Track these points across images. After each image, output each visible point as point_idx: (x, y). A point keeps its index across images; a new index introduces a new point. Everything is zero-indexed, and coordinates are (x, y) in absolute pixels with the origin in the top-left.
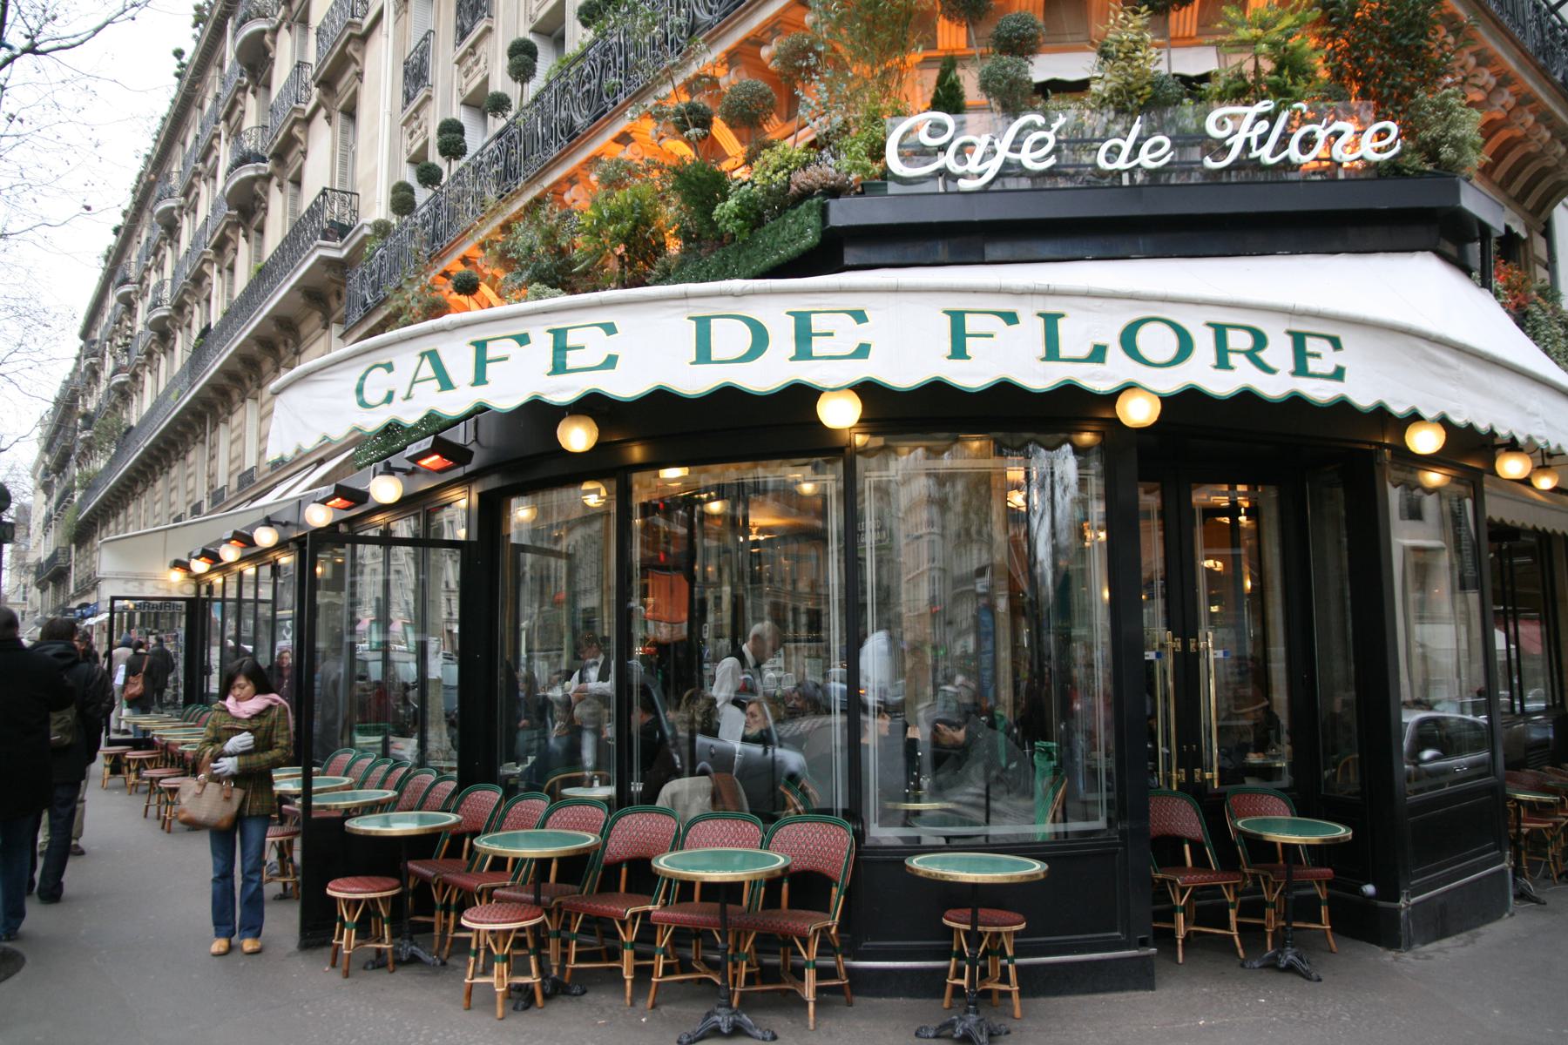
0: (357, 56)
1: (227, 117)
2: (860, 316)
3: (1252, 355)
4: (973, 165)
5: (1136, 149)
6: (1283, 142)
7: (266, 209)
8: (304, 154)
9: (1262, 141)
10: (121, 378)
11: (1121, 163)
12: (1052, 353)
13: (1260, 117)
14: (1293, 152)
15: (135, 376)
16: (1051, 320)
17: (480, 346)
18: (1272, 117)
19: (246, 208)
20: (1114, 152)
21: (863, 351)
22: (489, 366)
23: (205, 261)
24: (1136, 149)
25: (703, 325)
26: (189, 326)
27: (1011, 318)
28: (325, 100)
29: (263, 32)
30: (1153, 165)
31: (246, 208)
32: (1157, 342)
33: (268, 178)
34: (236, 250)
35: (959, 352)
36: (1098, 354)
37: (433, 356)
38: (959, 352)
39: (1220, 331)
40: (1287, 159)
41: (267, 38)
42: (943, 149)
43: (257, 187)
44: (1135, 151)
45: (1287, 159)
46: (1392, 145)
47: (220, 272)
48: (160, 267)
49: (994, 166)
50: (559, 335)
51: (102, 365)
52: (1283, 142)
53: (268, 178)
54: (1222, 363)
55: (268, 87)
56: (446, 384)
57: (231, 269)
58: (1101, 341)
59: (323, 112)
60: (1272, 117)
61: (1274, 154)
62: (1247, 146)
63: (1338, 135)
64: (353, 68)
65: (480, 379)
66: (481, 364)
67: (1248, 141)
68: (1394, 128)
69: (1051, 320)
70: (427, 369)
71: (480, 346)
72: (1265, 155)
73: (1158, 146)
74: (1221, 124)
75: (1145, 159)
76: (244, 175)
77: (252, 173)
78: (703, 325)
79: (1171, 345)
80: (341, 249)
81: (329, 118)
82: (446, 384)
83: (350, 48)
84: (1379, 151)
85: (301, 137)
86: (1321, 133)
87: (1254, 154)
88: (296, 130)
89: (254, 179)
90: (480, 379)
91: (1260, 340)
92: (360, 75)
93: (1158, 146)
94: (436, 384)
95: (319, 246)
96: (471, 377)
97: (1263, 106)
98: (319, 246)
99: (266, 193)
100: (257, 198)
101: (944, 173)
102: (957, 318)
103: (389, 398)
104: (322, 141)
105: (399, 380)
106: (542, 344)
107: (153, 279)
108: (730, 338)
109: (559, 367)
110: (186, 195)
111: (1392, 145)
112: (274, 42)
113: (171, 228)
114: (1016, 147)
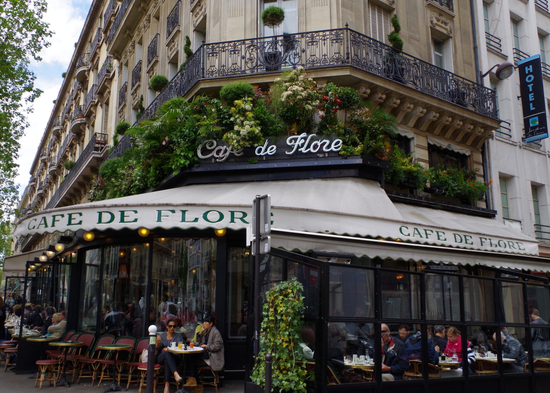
0: (109, 86)
1: (75, 98)
2: (136, 212)
3: (242, 219)
4: (221, 155)
5: (266, 150)
6: (309, 146)
7: (84, 135)
8: (95, 117)
9: (303, 145)
10: (41, 191)
11: (262, 154)
12: (183, 220)
13: (302, 138)
14: (311, 149)
15: (46, 191)
16: (184, 212)
17: (54, 217)
18: (305, 139)
19: (78, 133)
20: (260, 150)
21: (136, 220)
22: (56, 222)
23: (67, 151)
24: (266, 150)
25: (100, 214)
26: (62, 174)
27: (173, 211)
28: (100, 100)
29: (85, 71)
30: (271, 154)
31: (78, 133)
32: (213, 216)
33: (85, 124)
34: (76, 148)
35: (159, 220)
36: (196, 220)
37: (44, 218)
38: (159, 220)
39: (232, 213)
40: (310, 151)
41: (86, 73)
42: (213, 150)
43: (81, 127)
45: (310, 151)
46: (339, 147)
47: (71, 155)
48: (55, 151)
49: (228, 154)
50: (70, 215)
51: (36, 185)
52: (309, 146)
53: (85, 124)
54: (232, 221)
55: (87, 89)
57: (75, 154)
58: (197, 217)
59: (100, 103)
60: (305, 139)
61: (306, 149)
62: (299, 147)
63: (325, 143)
64: (108, 90)
65: (53, 225)
66: (54, 221)
67: (298, 145)
68: (341, 141)
69: (184, 212)
70: (43, 222)
71: (54, 217)
72: (303, 150)
73: (273, 148)
74: (291, 141)
75: (268, 152)
76: (77, 123)
77: (79, 122)
78: (100, 214)
79: (218, 216)
80: (101, 154)
81: (101, 106)
82: (46, 226)
83: (106, 83)
84: (336, 148)
85: (94, 111)
87: (300, 150)
88: (92, 109)
89: (80, 124)
90: (53, 225)
91: (245, 215)
92: (109, 92)
93: (273, 148)
94: (44, 225)
95: (93, 153)
96: (51, 225)
97: (304, 135)
98: (93, 153)
99: (85, 129)
100: (81, 130)
101: (213, 157)
102: (160, 212)
104: (100, 113)
105: (36, 224)
106: (67, 217)
107: (53, 155)
108: (106, 217)
109: (70, 223)
110: (63, 125)
111: (339, 147)
112: (89, 74)
113: (58, 136)
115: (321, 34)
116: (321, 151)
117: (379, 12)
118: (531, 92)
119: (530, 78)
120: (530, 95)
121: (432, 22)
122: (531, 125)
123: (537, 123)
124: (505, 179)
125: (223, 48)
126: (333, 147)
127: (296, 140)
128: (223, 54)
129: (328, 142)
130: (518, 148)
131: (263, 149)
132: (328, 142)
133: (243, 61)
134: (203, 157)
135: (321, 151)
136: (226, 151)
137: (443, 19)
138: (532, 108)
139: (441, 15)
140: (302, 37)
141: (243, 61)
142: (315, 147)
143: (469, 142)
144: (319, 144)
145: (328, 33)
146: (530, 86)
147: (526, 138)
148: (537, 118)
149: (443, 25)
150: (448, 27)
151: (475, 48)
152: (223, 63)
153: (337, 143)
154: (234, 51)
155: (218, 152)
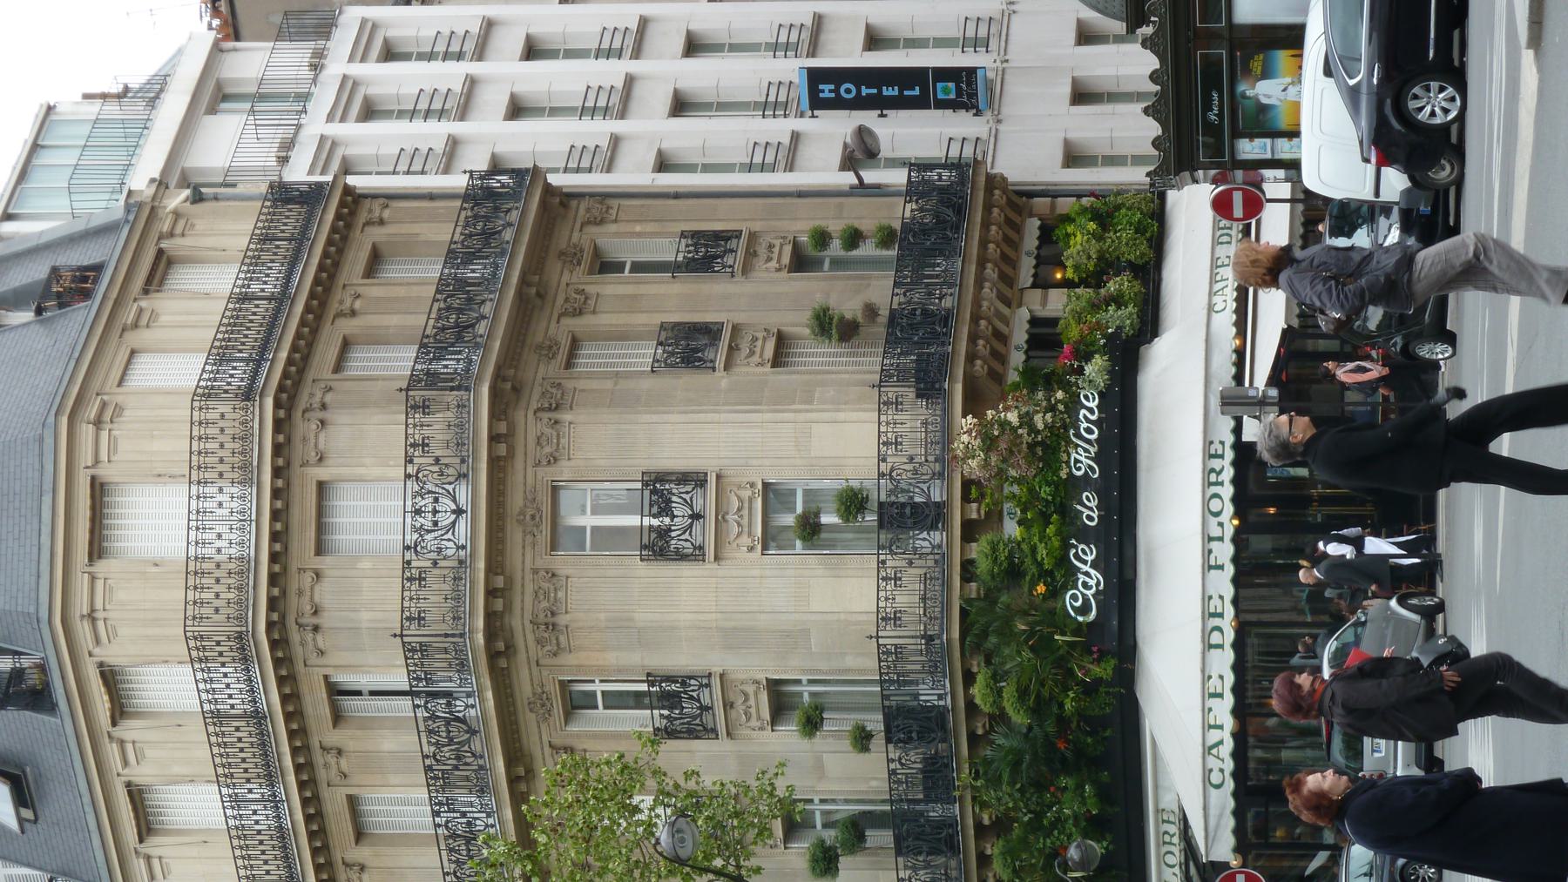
4: (1092, 583)
5: (1091, 509)
6: (1088, 441)
9: (1086, 450)
11: (1095, 515)
20: (1090, 518)
24: (1091, 509)
44: (1089, 509)
49: (1093, 572)
52: (1088, 441)
56: (1221, 742)
70: (1214, 751)
72: (1092, 450)
74: (1079, 469)
75: (1093, 504)
82: (1221, 742)
86: (1085, 425)
90: (1221, 727)
103: (1222, 770)
114: (1085, 562)
115: (883, 429)
116: (1097, 423)
117: (787, 355)
118: (880, 91)
119: (848, 91)
120: (885, 93)
121: (779, 270)
122: (953, 96)
123: (952, 85)
124: (1073, 157)
125: (887, 599)
126: (1093, 404)
127: (1077, 461)
128: (898, 599)
129: (1083, 411)
130: (1001, 127)
131: (1087, 512)
132: (1083, 411)
133: (917, 563)
134: (1094, 612)
135: (1097, 423)
136: (1087, 574)
137: (762, 251)
138: (917, 91)
139: (755, 254)
140: (884, 460)
141: (917, 563)
142: (1089, 431)
143: (1018, 220)
144: (1085, 425)
145: (883, 418)
146: (865, 91)
147: (977, 107)
148: (939, 85)
149: (776, 250)
150: (777, 243)
151: (801, 194)
152: (917, 599)
153: (1086, 398)
154: (896, 579)
155: (1085, 585)
